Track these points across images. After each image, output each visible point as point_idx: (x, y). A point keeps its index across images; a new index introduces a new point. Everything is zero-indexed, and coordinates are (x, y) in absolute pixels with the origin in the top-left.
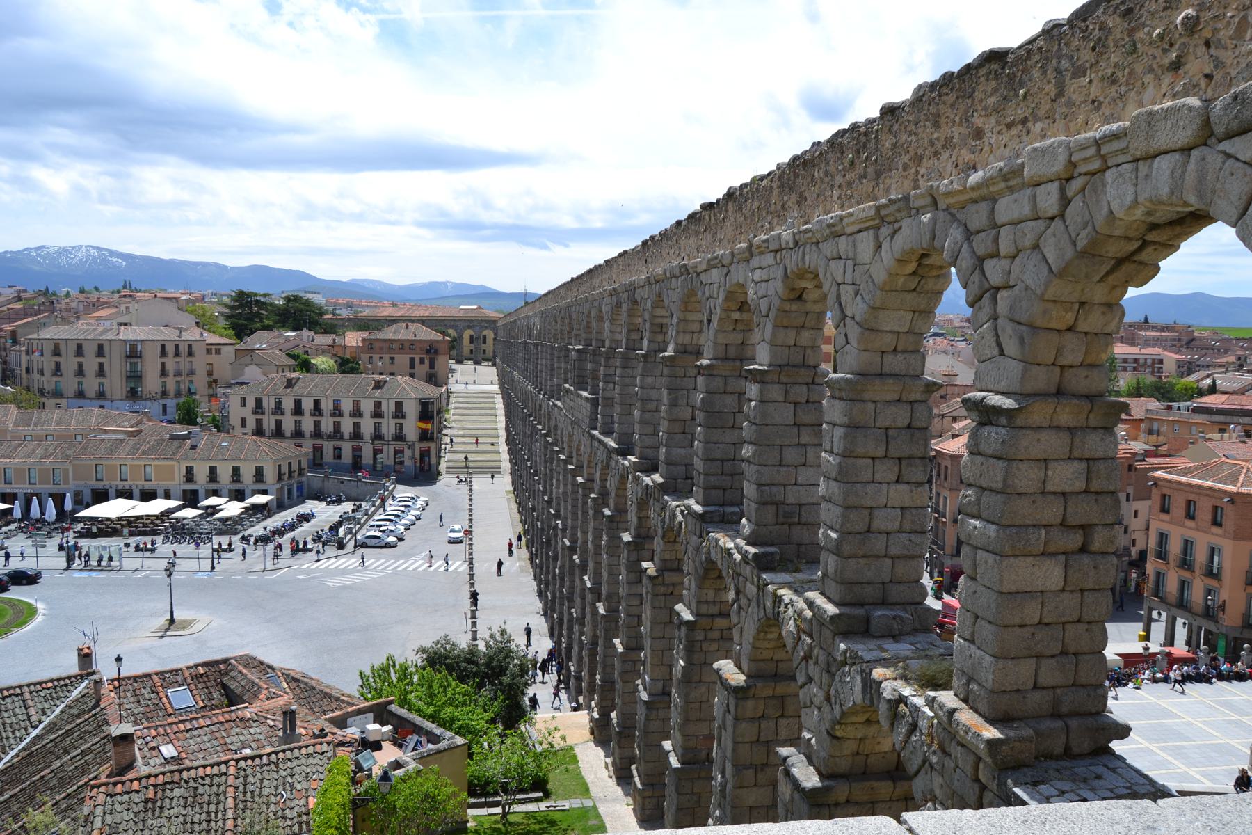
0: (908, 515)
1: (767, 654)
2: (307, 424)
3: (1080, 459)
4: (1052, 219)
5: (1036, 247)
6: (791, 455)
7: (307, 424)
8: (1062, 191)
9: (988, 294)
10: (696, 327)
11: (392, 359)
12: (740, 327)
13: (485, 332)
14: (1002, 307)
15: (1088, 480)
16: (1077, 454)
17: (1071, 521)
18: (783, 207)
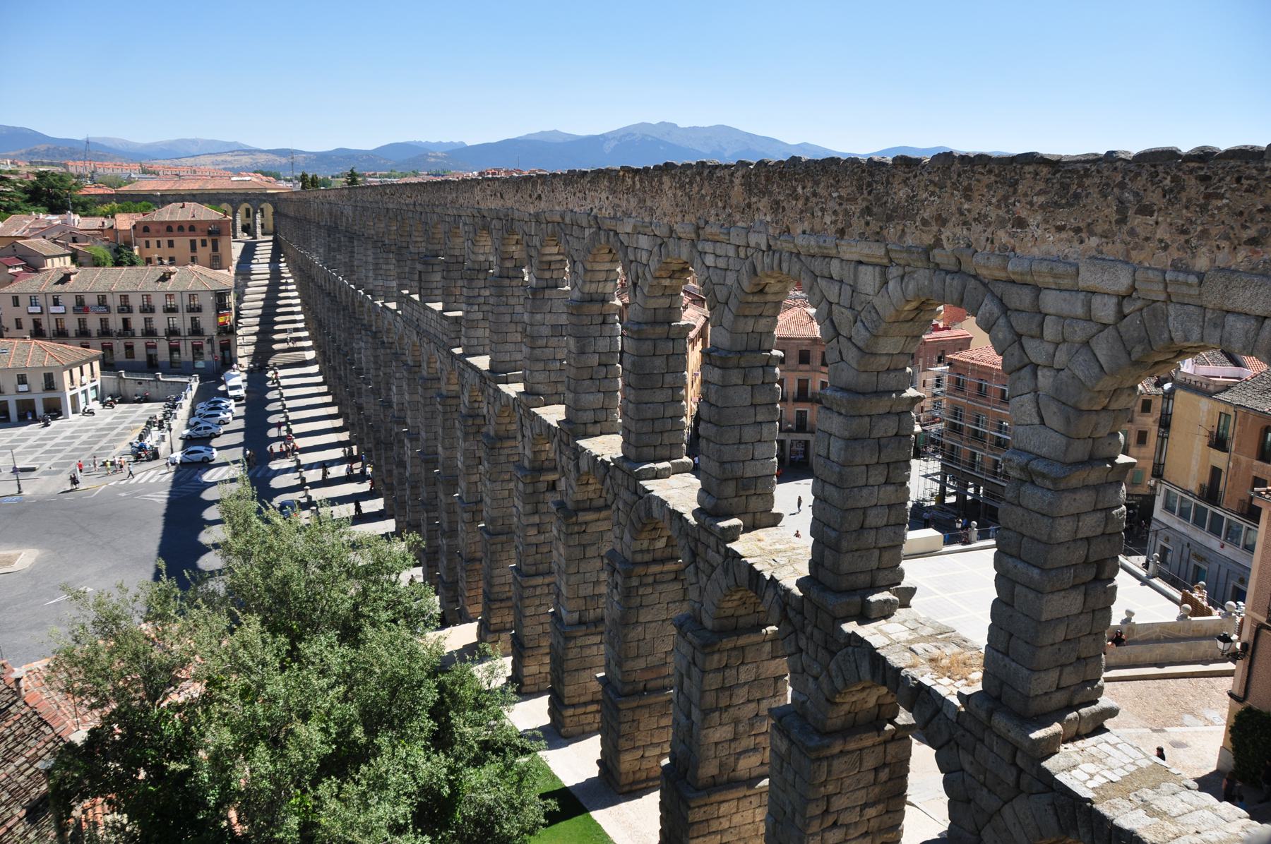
1: (729, 612)
2: (93, 323)
4: (1106, 326)
5: (1086, 344)
6: (749, 434)
7: (93, 323)
10: (602, 276)
11: (171, 244)
12: (669, 292)
13: (263, 206)
16: (1100, 506)
18: (749, 205)
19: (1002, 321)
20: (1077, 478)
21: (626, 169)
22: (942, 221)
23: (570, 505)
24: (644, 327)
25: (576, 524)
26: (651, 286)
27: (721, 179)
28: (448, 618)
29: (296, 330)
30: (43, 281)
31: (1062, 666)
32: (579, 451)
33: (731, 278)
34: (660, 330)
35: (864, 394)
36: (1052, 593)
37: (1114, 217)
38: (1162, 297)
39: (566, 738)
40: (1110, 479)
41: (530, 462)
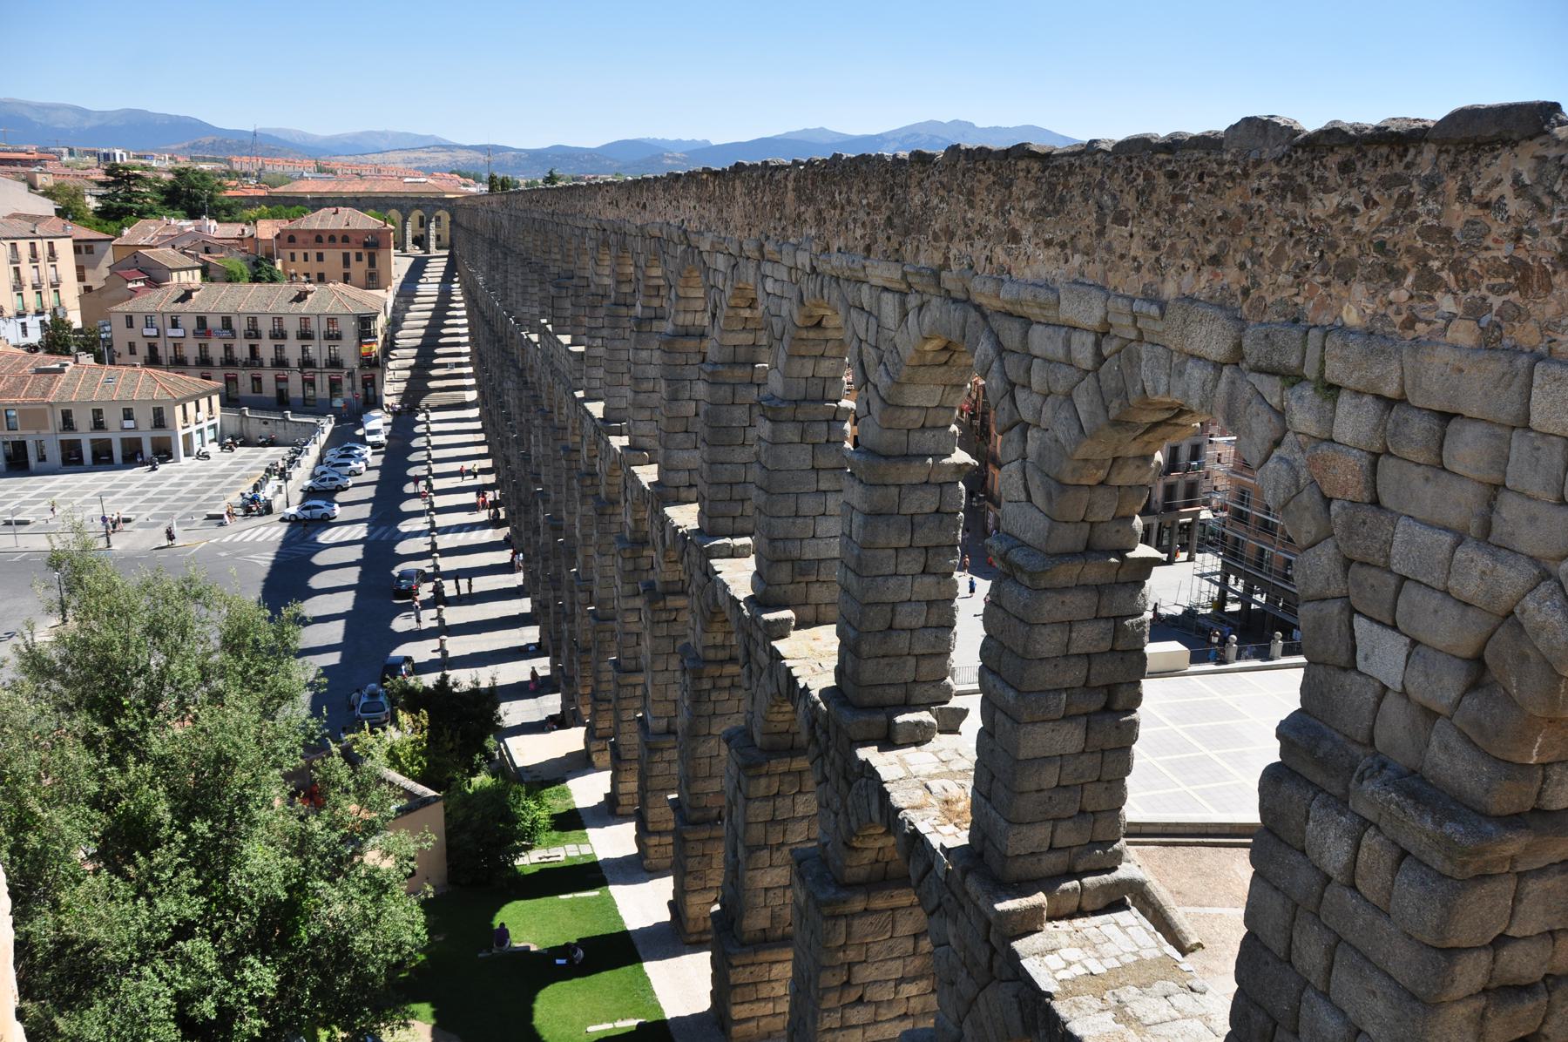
0: (934, 610)
2: (216, 350)
3: (1107, 618)
4: (1088, 372)
6: (809, 505)
7: (216, 350)
8: (1098, 345)
9: (1017, 429)
11: (320, 257)
13: (439, 213)
14: (1032, 447)
15: (1115, 639)
16: (1104, 613)
17: (1094, 683)
18: (799, 216)
19: (995, 365)
20: (1066, 573)
21: (707, 170)
22: (950, 235)
23: (658, 587)
24: (720, 368)
25: (665, 609)
26: (727, 317)
27: (779, 182)
28: (569, 720)
29: (459, 365)
30: (162, 298)
31: (1056, 820)
32: (665, 520)
33: (785, 307)
34: (740, 373)
35: (887, 457)
36: (1034, 723)
37: (1095, 228)
38: (1133, 335)
39: (649, 871)
40: (1122, 577)
41: (632, 532)
